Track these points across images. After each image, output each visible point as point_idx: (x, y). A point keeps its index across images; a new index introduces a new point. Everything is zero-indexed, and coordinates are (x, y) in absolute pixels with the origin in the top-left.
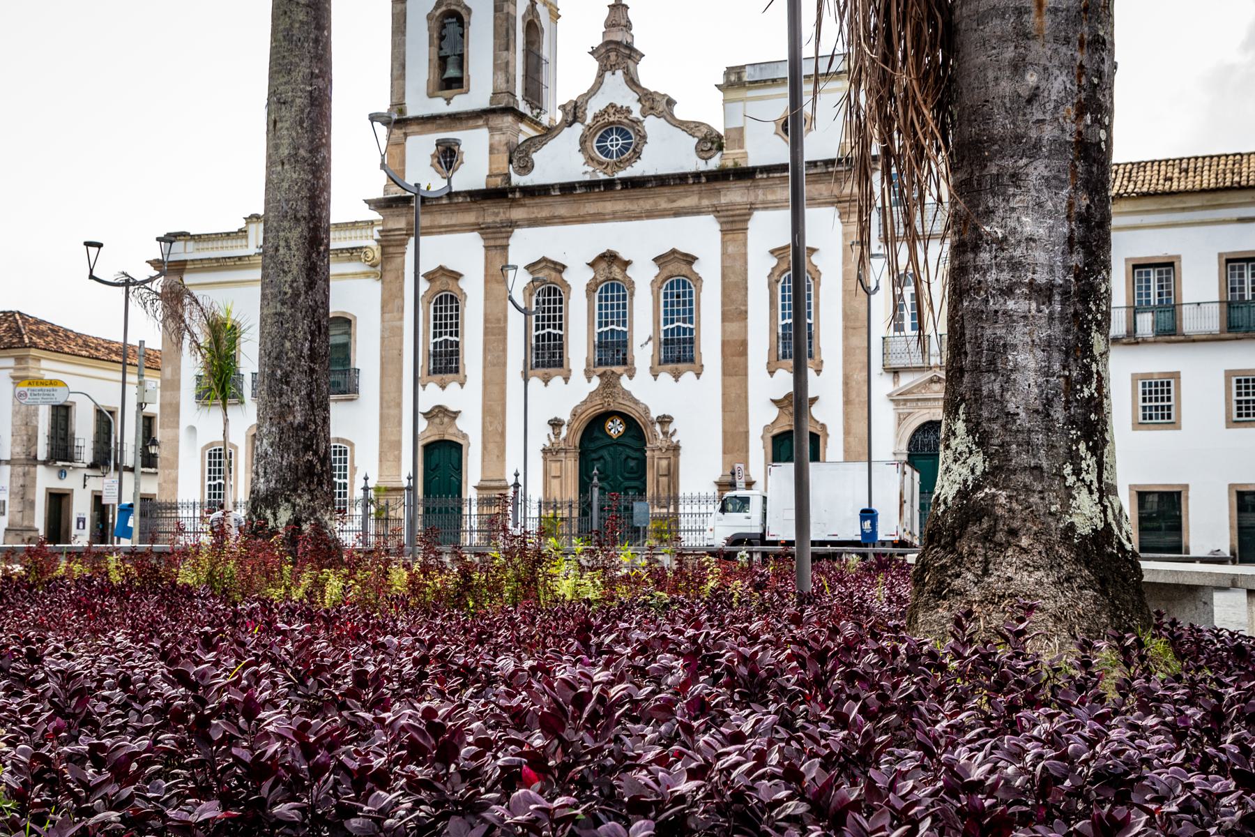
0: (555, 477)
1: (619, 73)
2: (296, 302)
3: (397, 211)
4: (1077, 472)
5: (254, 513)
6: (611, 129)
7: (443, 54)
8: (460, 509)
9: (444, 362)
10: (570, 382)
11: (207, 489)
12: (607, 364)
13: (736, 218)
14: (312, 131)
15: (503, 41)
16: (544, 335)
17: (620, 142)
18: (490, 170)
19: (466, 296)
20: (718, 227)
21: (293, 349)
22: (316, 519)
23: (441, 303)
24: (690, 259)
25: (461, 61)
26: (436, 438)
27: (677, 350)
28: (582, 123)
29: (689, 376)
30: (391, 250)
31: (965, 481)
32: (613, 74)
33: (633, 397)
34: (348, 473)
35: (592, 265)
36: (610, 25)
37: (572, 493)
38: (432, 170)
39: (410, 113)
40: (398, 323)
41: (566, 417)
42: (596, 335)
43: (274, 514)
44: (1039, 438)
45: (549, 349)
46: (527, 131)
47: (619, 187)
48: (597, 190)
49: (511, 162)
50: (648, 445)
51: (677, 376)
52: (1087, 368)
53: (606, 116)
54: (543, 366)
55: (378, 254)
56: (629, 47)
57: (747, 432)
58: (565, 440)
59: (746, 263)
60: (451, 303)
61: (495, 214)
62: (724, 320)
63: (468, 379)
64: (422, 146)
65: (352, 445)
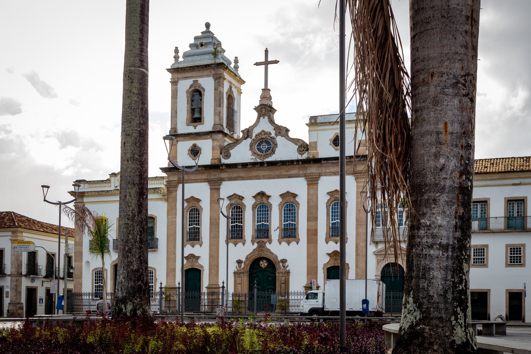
0: (239, 284)
1: (266, 118)
2: (134, 219)
3: (173, 173)
4: (456, 319)
5: (117, 306)
6: (263, 141)
7: (193, 107)
8: (200, 297)
9: (193, 236)
10: (245, 245)
11: (94, 287)
12: (260, 238)
13: (313, 179)
14: (140, 147)
15: (218, 103)
16: (234, 226)
17: (267, 146)
18: (213, 156)
19: (202, 209)
20: (306, 183)
21: (133, 238)
22: (143, 309)
23: (192, 212)
24: (295, 196)
25: (200, 111)
26: (190, 267)
27: (289, 232)
28: (251, 138)
29: (294, 244)
30: (171, 189)
31: (412, 322)
32: (264, 118)
33: (271, 252)
34: (154, 281)
35: (254, 197)
36: (263, 97)
37: (246, 290)
38: (188, 156)
39: (180, 132)
40: (174, 220)
41: (244, 259)
42: (256, 226)
43: (125, 307)
44: (442, 306)
45: (237, 231)
46: (228, 141)
47: (266, 165)
48: (257, 166)
49: (221, 153)
50: (277, 271)
51: (289, 243)
52: (461, 278)
53: (261, 135)
54: (234, 238)
55: (166, 191)
56: (271, 107)
57: (317, 267)
58: (243, 268)
59: (317, 197)
60: (196, 212)
61: (215, 175)
62: (308, 221)
63: (203, 243)
64: (184, 146)
65: (155, 270)
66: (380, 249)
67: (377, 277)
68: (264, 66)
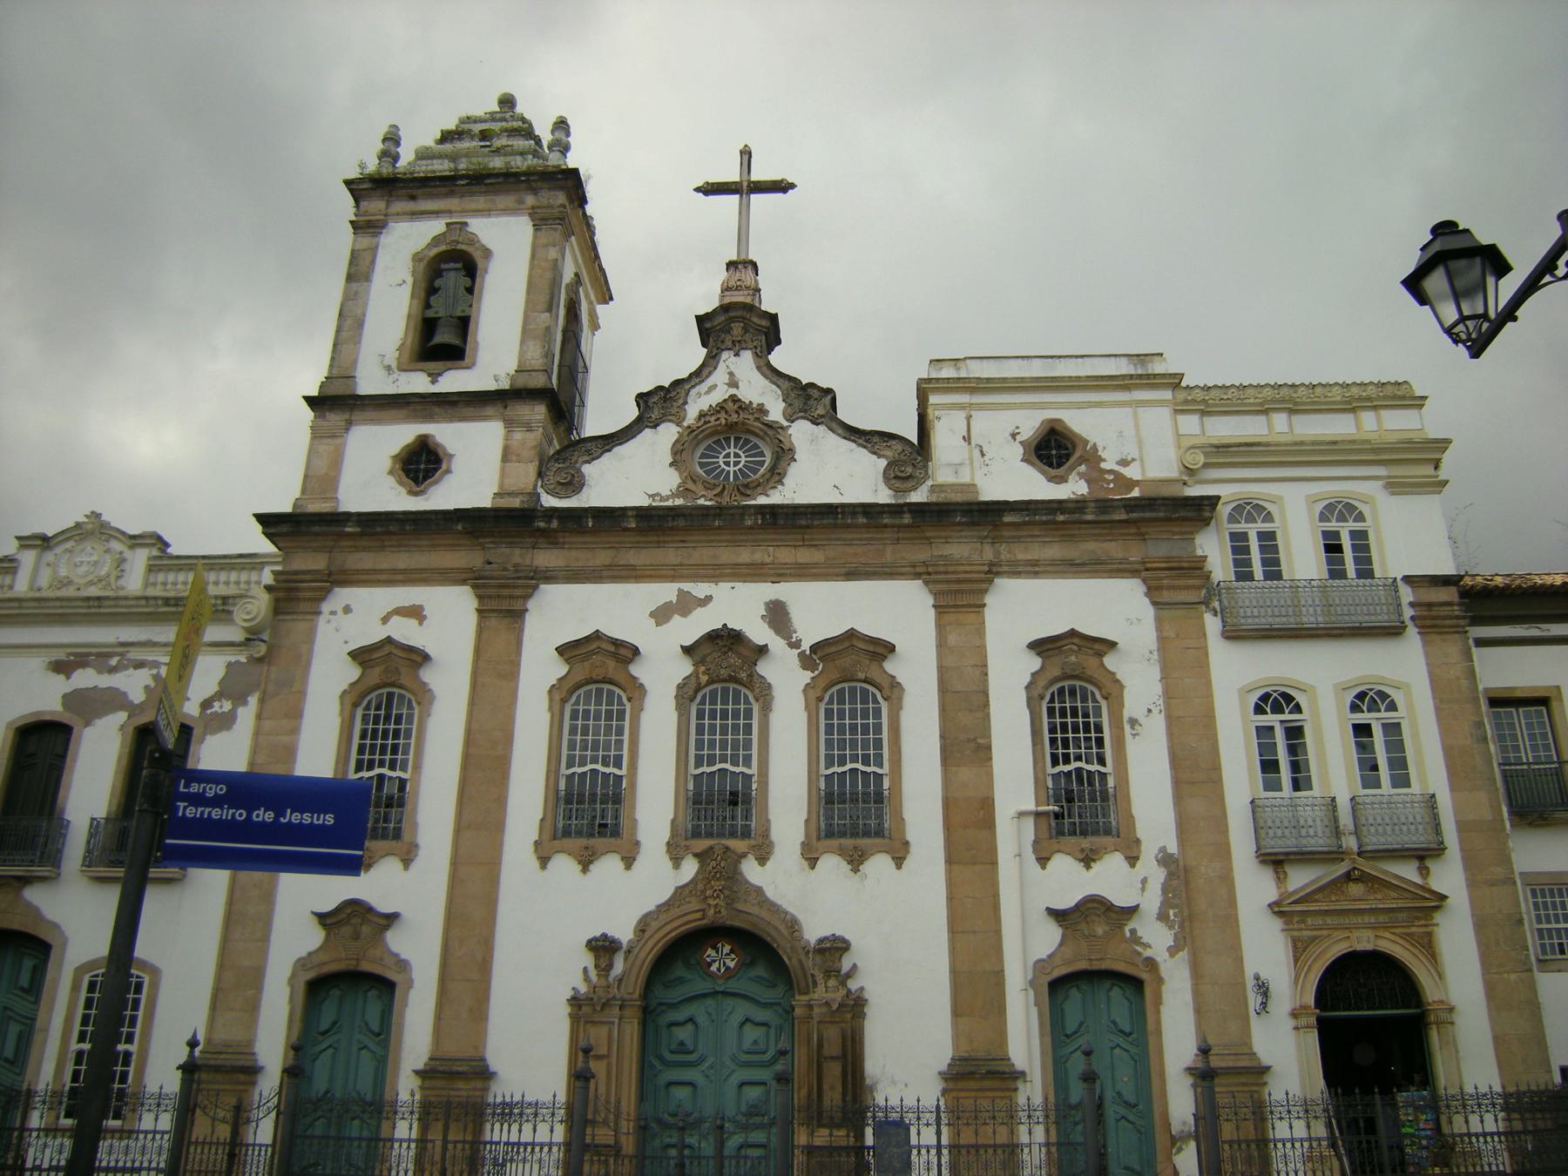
7: (430, 314)
10: (637, 865)
17: (743, 459)
18: (501, 485)
20: (930, 600)
24: (883, 650)
28: (678, 424)
29: (879, 864)
32: (737, 355)
33: (767, 900)
41: (624, 932)
51: (856, 861)
66: (1295, 892)
67: (1303, 1021)
68: (736, 197)
